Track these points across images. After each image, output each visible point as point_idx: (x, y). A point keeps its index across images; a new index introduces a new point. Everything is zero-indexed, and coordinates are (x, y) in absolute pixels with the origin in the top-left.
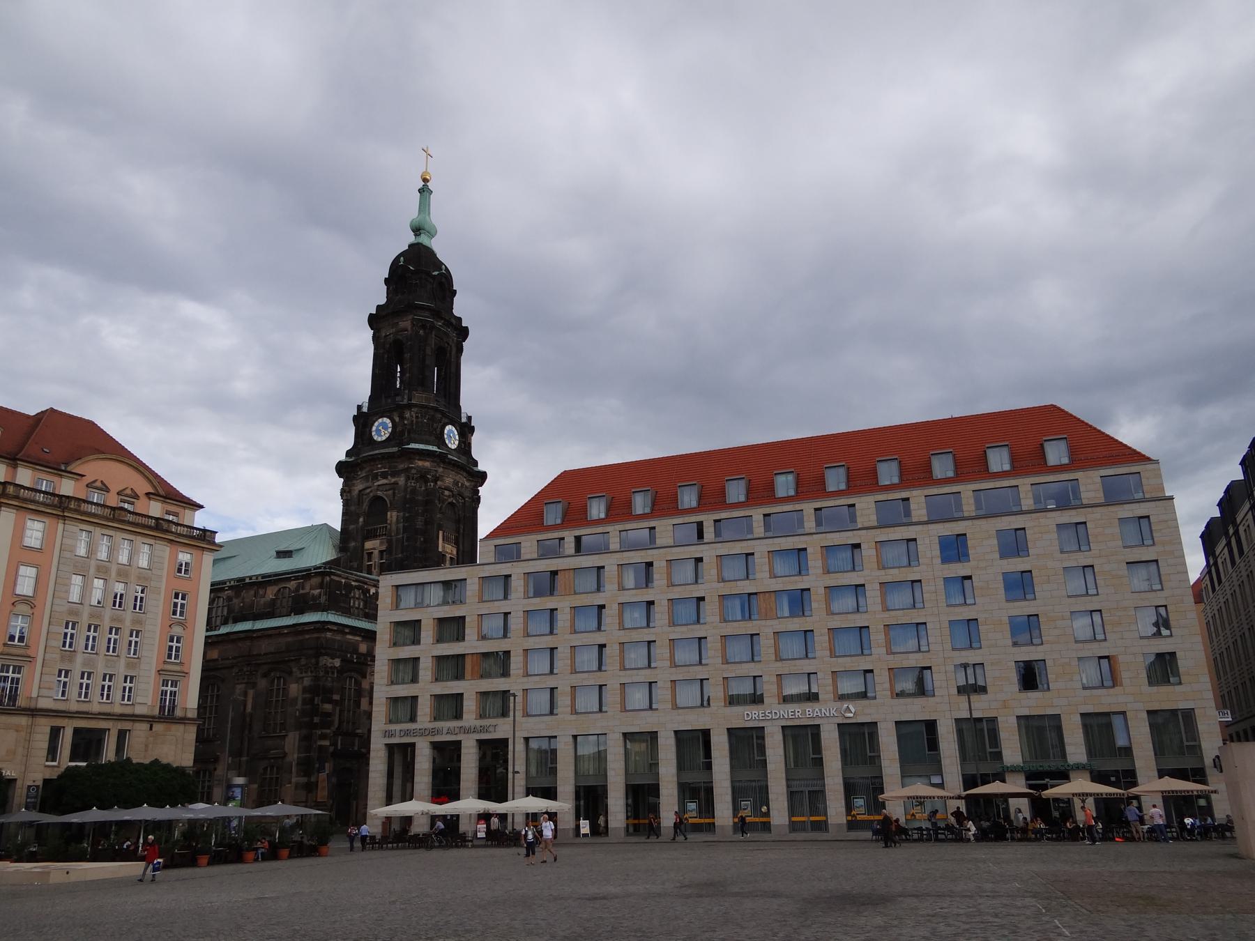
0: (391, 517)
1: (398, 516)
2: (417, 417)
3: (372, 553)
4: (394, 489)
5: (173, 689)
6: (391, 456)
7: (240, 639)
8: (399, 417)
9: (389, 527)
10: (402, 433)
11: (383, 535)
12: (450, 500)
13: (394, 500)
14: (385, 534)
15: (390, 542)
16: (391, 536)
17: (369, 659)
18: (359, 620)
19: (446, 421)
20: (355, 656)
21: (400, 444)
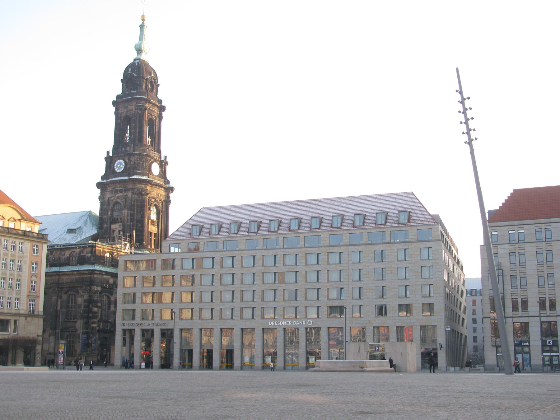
0: (124, 213)
1: (128, 213)
2: (137, 160)
3: (115, 231)
4: (126, 199)
5: (34, 303)
6: (125, 181)
7: (53, 275)
8: (128, 160)
9: (123, 218)
10: (130, 168)
11: (120, 222)
12: (155, 203)
13: (126, 204)
14: (122, 222)
15: (124, 226)
16: (125, 223)
17: (114, 286)
18: (109, 268)
19: (153, 160)
20: (108, 285)
21: (129, 175)
